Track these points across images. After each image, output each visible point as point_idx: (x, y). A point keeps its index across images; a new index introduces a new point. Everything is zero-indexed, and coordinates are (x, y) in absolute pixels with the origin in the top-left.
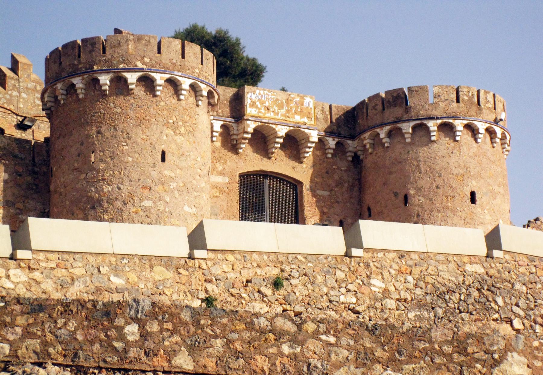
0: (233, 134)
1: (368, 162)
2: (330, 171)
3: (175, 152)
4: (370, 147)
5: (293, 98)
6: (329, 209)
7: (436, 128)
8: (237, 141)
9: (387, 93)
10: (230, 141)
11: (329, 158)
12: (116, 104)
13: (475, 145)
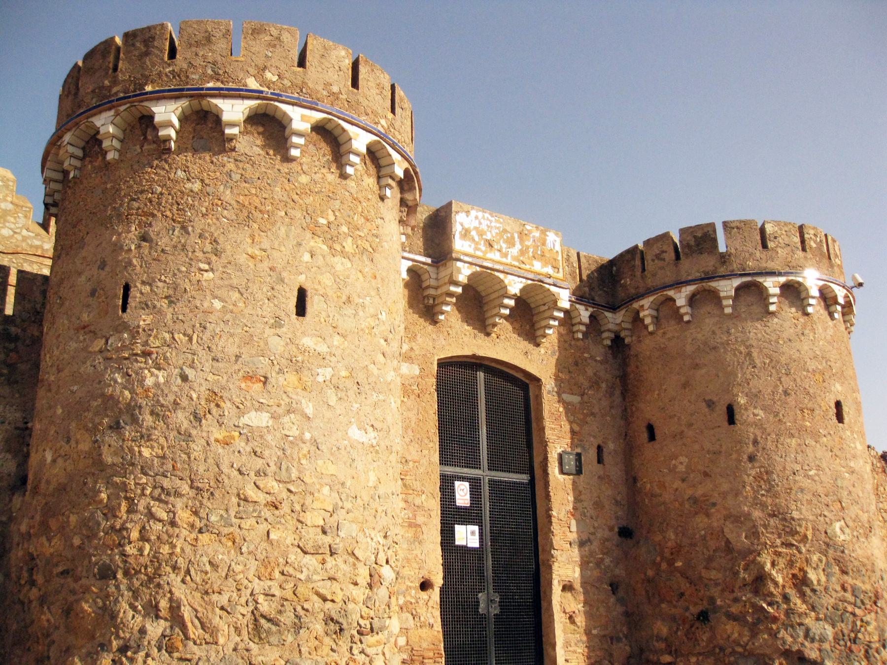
0: (428, 287)
1: (646, 347)
2: (580, 361)
3: (330, 292)
4: (652, 322)
5: (530, 232)
6: (581, 426)
7: (777, 291)
8: (434, 299)
9: (683, 231)
10: (423, 299)
11: (578, 339)
12: (190, 172)
13: (831, 323)
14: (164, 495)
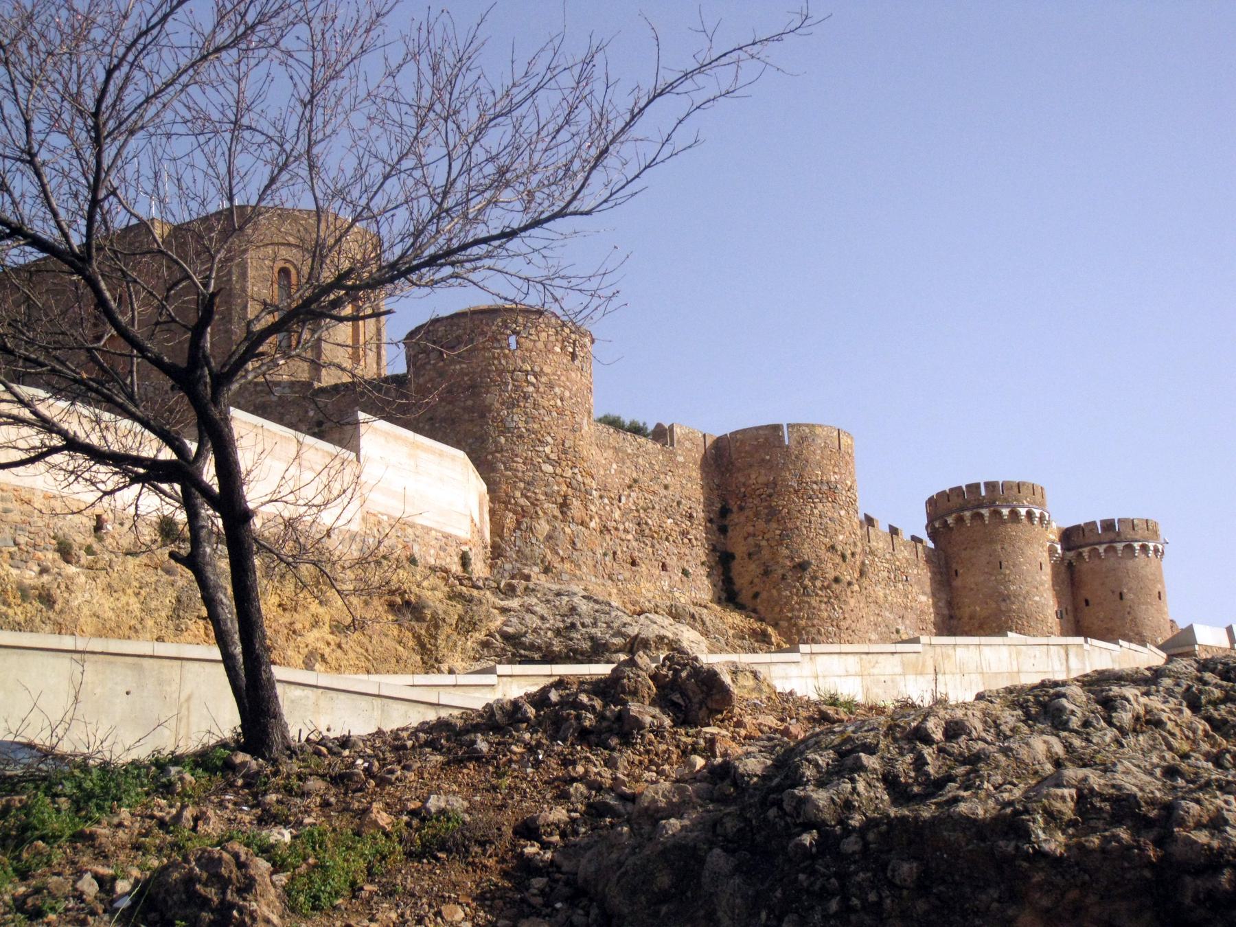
1: (1085, 567)
12: (1011, 529)
14: (1020, 618)
